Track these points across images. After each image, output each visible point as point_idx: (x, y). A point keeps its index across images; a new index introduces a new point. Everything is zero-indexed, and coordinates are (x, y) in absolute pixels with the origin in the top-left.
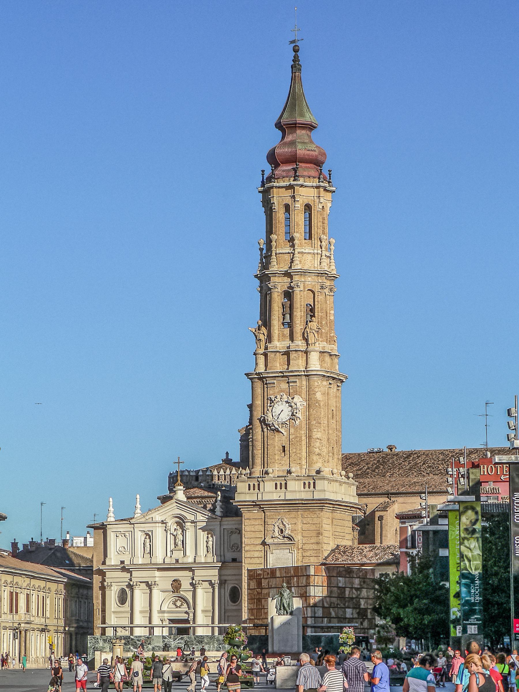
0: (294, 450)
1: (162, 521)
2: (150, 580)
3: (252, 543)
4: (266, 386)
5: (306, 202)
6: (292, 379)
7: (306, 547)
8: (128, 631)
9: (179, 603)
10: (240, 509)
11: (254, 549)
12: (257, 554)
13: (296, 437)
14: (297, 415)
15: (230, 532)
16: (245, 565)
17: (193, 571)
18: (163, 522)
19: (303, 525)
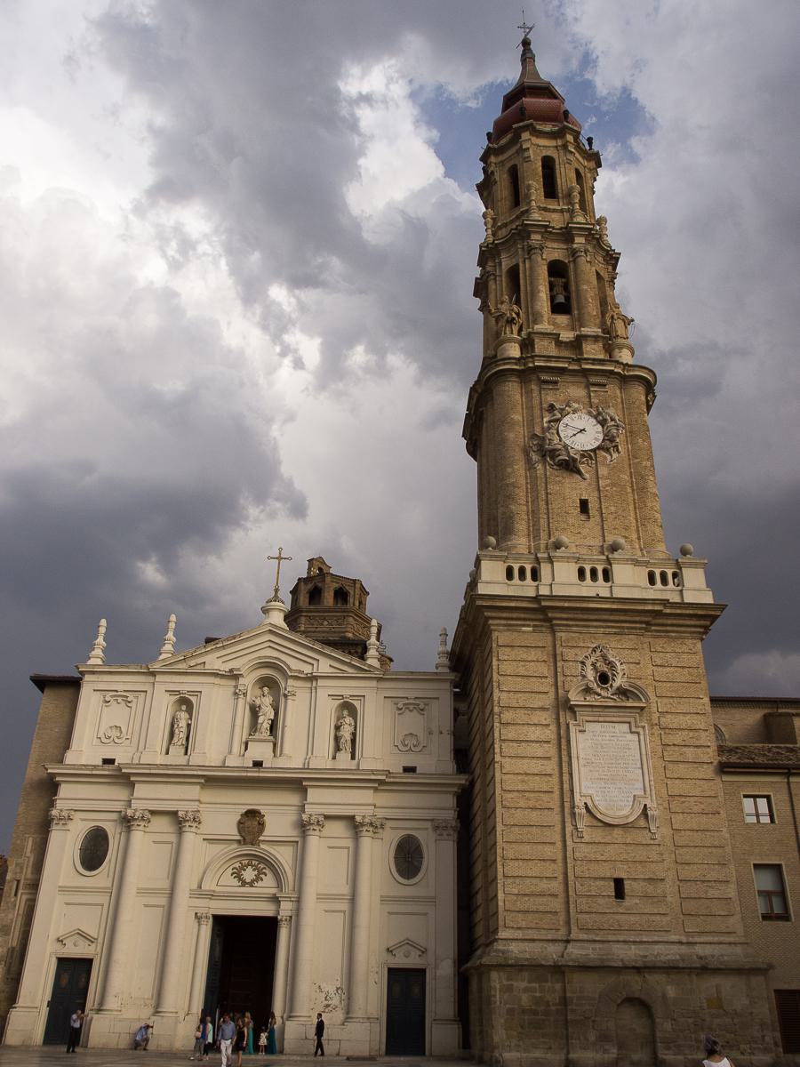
0: (613, 509)
1: (231, 671)
2: (182, 808)
3: (521, 705)
4: (533, 387)
5: (577, 166)
6: (593, 379)
7: (665, 721)
8: (94, 944)
9: (249, 874)
10: (488, 618)
11: (525, 719)
12: (535, 733)
13: (613, 485)
14: (618, 440)
15: (400, 706)
16: (504, 760)
17: (304, 791)
18: (233, 676)
19: (655, 668)
